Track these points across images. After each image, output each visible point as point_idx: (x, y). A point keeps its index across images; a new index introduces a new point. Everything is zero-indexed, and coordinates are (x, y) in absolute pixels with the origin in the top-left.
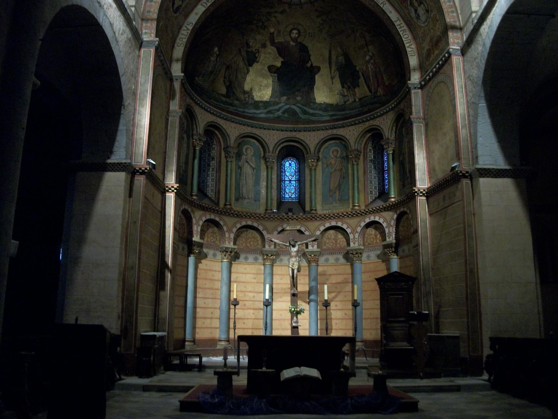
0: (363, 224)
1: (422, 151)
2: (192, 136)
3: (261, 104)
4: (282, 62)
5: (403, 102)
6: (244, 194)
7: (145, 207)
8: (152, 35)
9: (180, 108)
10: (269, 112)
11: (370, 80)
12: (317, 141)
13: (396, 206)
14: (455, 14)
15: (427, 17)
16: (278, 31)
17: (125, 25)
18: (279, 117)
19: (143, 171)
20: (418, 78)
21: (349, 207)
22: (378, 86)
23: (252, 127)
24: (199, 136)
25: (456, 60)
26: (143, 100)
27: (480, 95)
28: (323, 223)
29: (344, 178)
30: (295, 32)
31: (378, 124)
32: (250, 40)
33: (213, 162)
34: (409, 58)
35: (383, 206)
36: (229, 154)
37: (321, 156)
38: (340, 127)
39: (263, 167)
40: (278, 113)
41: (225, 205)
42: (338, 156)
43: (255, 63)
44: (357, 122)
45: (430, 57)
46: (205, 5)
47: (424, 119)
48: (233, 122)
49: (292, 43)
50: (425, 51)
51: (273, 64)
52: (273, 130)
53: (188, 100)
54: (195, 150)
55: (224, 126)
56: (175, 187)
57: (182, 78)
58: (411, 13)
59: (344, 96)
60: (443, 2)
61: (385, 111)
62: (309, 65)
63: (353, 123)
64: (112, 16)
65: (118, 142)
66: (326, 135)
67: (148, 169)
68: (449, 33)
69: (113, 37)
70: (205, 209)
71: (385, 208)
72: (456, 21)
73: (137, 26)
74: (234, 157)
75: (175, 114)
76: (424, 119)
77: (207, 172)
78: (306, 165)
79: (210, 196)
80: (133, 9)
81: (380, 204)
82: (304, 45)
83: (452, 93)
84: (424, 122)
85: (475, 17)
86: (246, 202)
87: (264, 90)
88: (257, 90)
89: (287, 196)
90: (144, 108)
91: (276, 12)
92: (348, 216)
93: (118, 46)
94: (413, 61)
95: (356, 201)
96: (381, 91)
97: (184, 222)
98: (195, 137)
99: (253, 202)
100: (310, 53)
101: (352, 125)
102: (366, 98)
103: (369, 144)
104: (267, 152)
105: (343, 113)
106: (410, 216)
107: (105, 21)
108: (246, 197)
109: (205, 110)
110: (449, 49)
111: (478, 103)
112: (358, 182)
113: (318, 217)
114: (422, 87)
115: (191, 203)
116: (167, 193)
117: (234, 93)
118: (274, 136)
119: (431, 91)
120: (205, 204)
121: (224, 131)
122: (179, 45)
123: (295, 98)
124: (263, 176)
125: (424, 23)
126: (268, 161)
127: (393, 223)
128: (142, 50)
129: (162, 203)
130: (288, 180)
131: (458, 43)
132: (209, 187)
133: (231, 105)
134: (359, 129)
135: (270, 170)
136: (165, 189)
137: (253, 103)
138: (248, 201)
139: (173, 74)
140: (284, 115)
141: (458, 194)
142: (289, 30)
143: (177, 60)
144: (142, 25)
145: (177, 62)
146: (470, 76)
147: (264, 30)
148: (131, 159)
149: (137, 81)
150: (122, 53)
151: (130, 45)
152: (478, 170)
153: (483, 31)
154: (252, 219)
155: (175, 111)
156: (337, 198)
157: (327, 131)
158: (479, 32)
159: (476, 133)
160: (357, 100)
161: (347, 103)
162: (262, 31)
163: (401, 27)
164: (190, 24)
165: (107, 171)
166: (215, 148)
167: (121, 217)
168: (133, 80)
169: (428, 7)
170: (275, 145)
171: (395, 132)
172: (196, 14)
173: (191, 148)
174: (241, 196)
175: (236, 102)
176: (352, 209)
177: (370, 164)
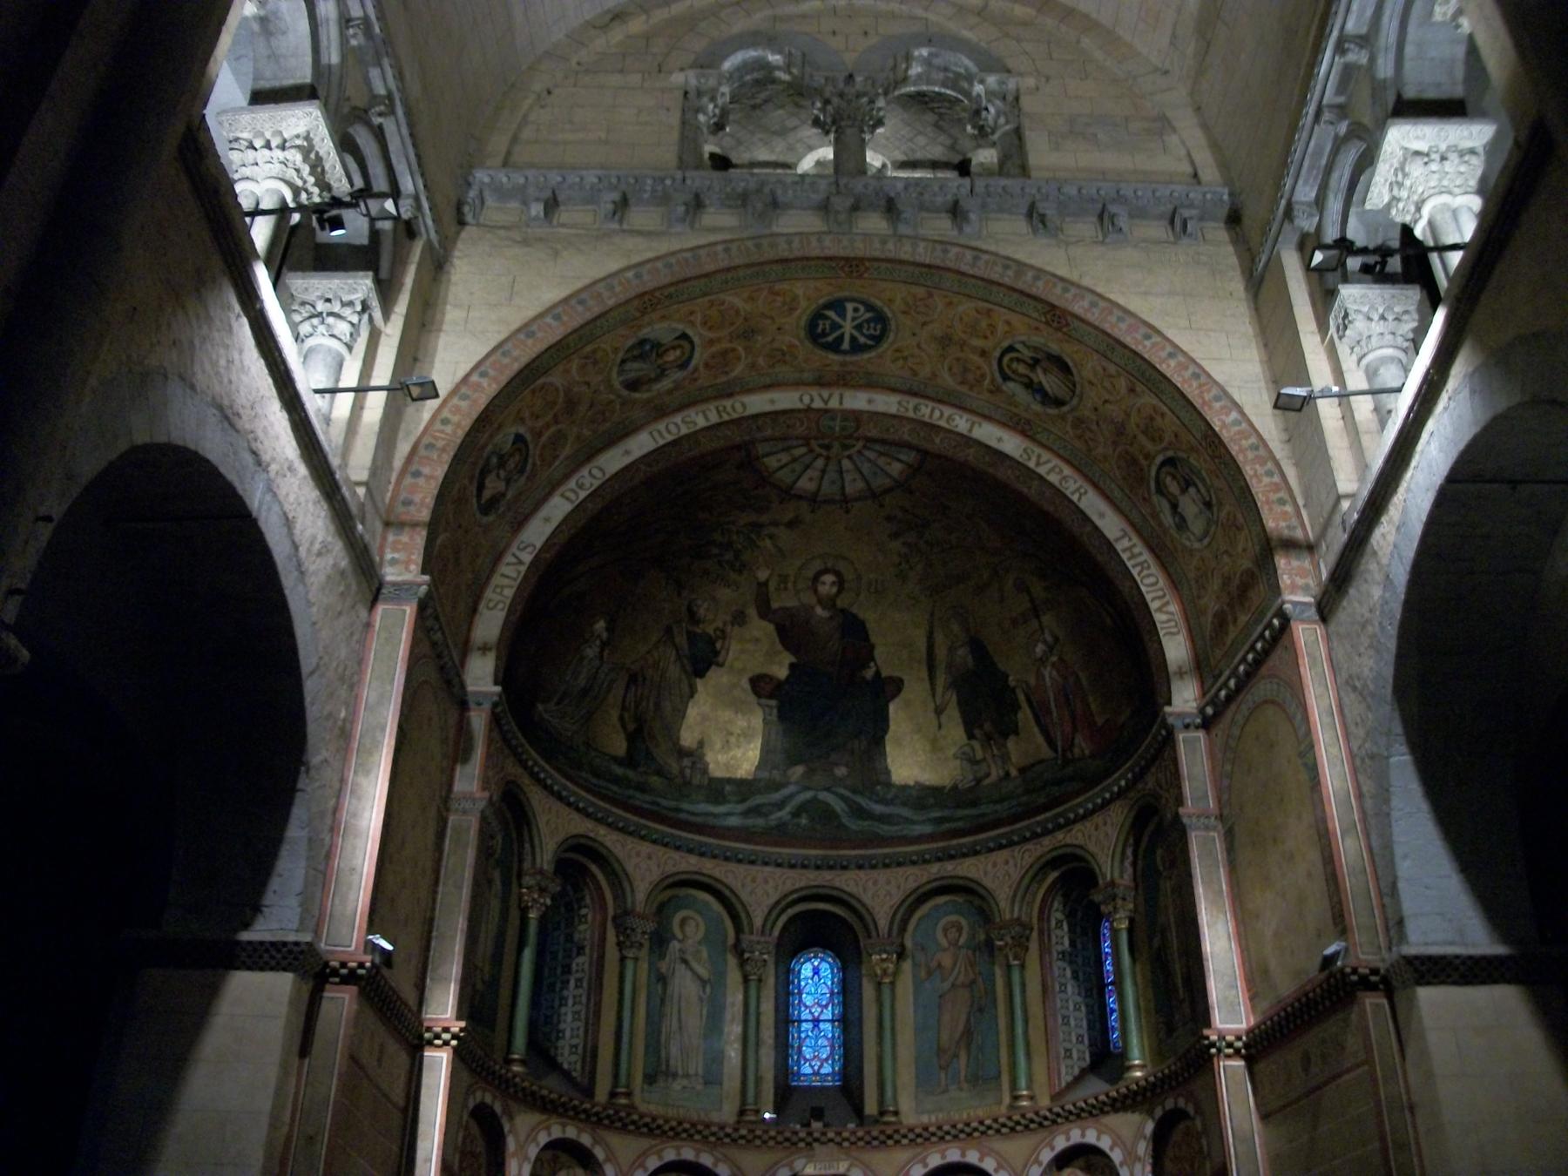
0: (1047, 1156)
1: (1222, 916)
2: (520, 876)
4: (792, 666)
5: (1153, 770)
6: (672, 1062)
7: (349, 1087)
8: (413, 567)
9: (484, 789)
10: (756, 811)
11: (1049, 712)
12: (896, 899)
13: (1149, 1094)
14: (1289, 508)
15: (1209, 522)
16: (780, 576)
17: (332, 528)
18: (782, 826)
19: (352, 972)
20: (1192, 697)
21: (1000, 1103)
22: (1075, 729)
23: (702, 855)
24: (539, 877)
25: (1306, 635)
26: (370, 753)
27: (1390, 730)
28: (919, 1154)
29: (981, 1010)
30: (829, 578)
31: (1082, 843)
32: (699, 602)
33: (581, 959)
34: (1165, 640)
35: (1107, 1095)
36: (628, 936)
37: (909, 944)
38: (965, 855)
39: (734, 976)
40: (779, 814)
41: (613, 1095)
42: (962, 941)
43: (713, 667)
44: (1016, 838)
45: (1227, 634)
46: (572, 496)
47: (1221, 817)
48: (643, 838)
49: (819, 611)
50: (1210, 619)
51: (765, 670)
52: (766, 864)
53: (513, 769)
54: (524, 920)
55: (618, 850)
56: (455, 1030)
57: (496, 698)
59: (973, 762)
60: (1251, 478)
61: (1099, 801)
62: (869, 674)
63: (1004, 842)
64: (292, 498)
65: (281, 876)
66: (925, 880)
67: (368, 964)
68: (1277, 558)
69: (289, 558)
70: (549, 1106)
71: (1115, 1100)
72: (1295, 528)
73: (367, 537)
74: (647, 945)
75: (468, 805)
76: (1221, 815)
77: (562, 989)
78: (864, 972)
79: (566, 1066)
80: (361, 491)
81: (1096, 1088)
82: (854, 616)
83: (1302, 731)
84: (1220, 827)
85: (1350, 510)
86: (679, 1088)
87: (739, 747)
88: (718, 746)
89: (806, 1069)
90: (372, 776)
91: (775, 524)
92: (998, 1131)
93: (305, 585)
94: (1176, 649)
95: (1023, 1082)
96: (1083, 745)
97: (480, 1147)
98: (528, 880)
99: (699, 1087)
100: (873, 639)
101: (1001, 847)
103: (1056, 905)
104: (746, 929)
105: (974, 812)
106: (1198, 1123)
107: (269, 509)
108: (680, 1072)
109: (560, 798)
110: (1283, 603)
111: (1386, 754)
112: (1026, 1021)
113: (905, 1136)
114: (1207, 724)
115: (504, 1086)
116: (427, 1048)
118: (766, 882)
119: (1236, 732)
120: (550, 1092)
121: (616, 865)
122: (491, 605)
124: (733, 1004)
125: (1201, 540)
127: (1143, 1148)
128: (380, 608)
129: (410, 1080)
130: (810, 1017)
131: (1306, 589)
132: (563, 1037)
133: (642, 788)
135: (753, 985)
136: (421, 1037)
137: (706, 782)
138: (685, 1082)
139: (470, 688)
140: (796, 820)
141: (1352, 1043)
142: (810, 573)
143: (484, 649)
144: (384, 538)
145: (484, 654)
146: (1351, 676)
147: (740, 572)
148: (317, 932)
149: (356, 697)
150: (314, 609)
151: (342, 588)
152: (1410, 961)
153: (1382, 542)
154: (697, 1141)
155: (469, 797)
156: (963, 1073)
157: (927, 867)
158: (1369, 547)
159: (1388, 846)
160: (1014, 772)
161: (987, 782)
162: (733, 576)
163: (1133, 557)
164: (525, 548)
165: (238, 968)
167: (264, 1121)
168: (343, 692)
171: (1134, 864)
172: (547, 520)
173: (514, 914)
174: (664, 1067)
175: (655, 781)
176: (1012, 1107)
177: (1060, 963)
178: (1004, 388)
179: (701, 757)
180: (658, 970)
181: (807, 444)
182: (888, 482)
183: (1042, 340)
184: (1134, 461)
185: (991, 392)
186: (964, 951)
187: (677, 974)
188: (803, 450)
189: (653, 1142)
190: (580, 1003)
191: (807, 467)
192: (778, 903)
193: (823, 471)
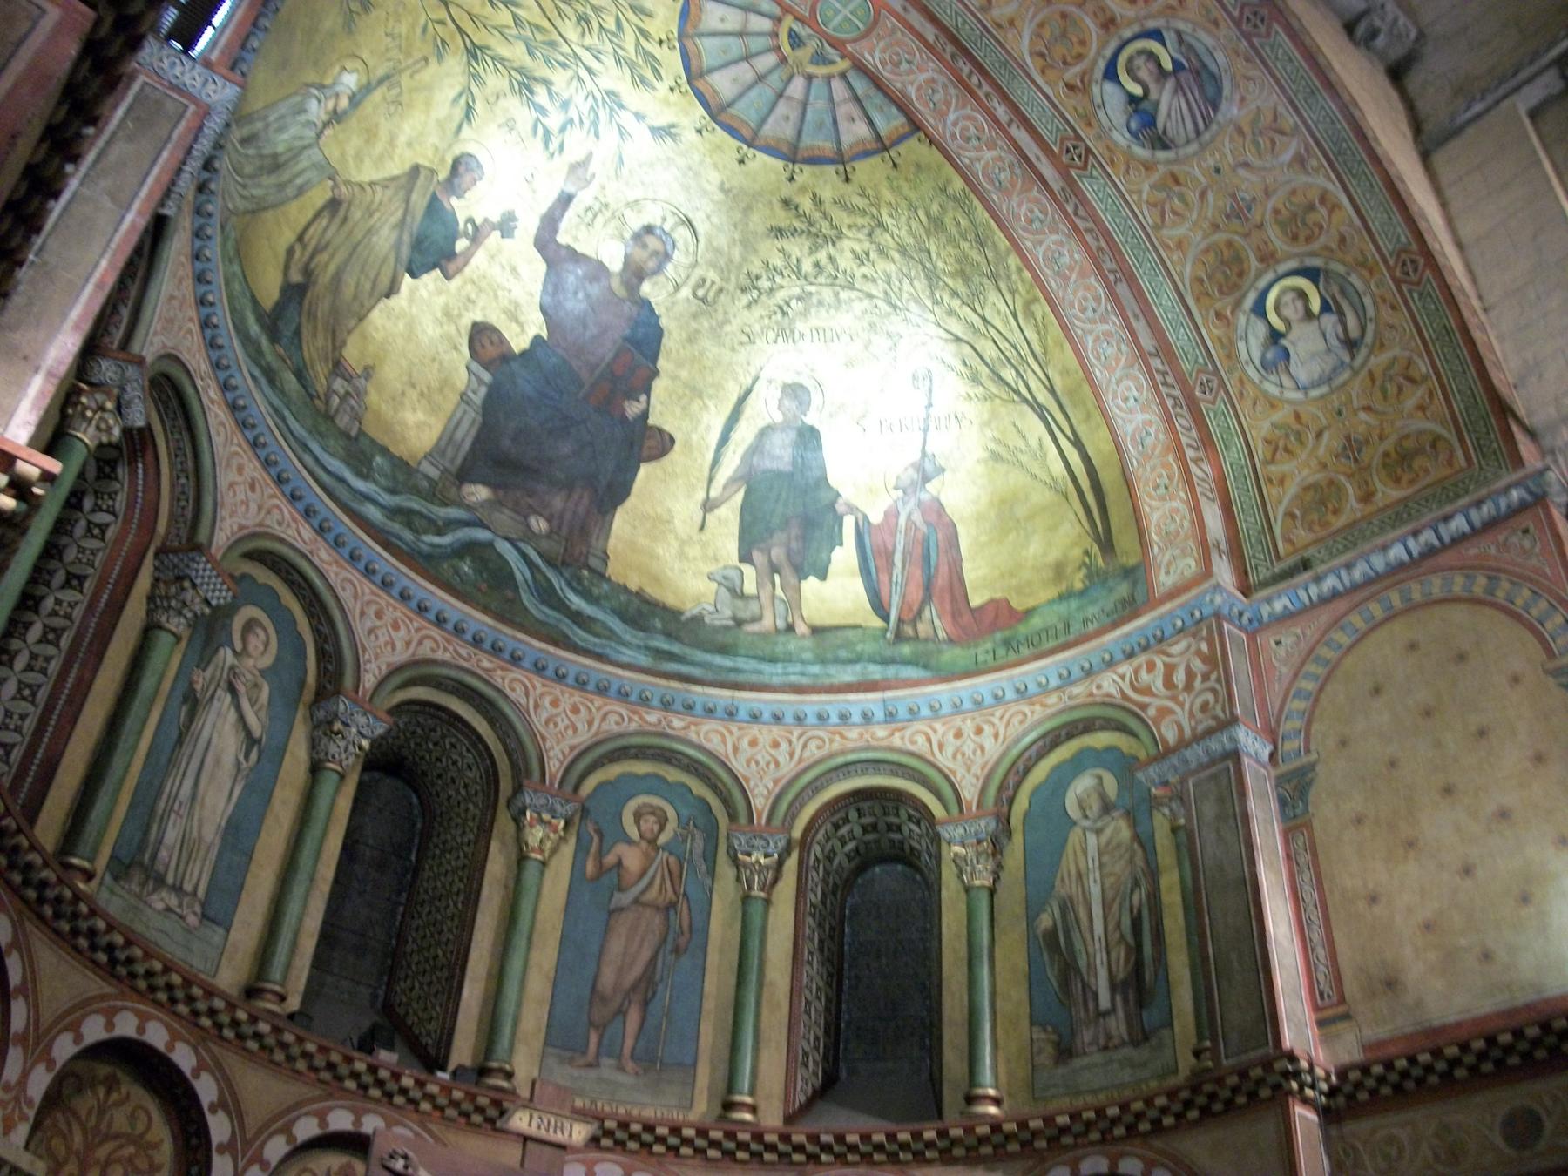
3: (378, 460)
6: (163, 853)
11: (891, 564)
12: (583, 737)
22: (923, 603)
29: (677, 951)
31: (921, 745)
33: (69, 596)
40: (437, 540)
42: (662, 840)
43: (438, 271)
49: (616, 284)
58: (1241, 345)
66: (633, 727)
86: (160, 906)
92: (700, 1152)
99: (192, 920)
100: (662, 363)
102: (851, 634)
103: (820, 836)
108: (170, 879)
117: (298, 333)
123: (526, 517)
126: (339, 732)
134: (805, 746)
137: (353, 433)
138: (173, 901)
154: (179, 1016)
160: (801, 628)
161: (754, 628)
166: (110, 533)
169: (1363, 329)
170: (391, 674)
178: (1096, 89)
179: (360, 394)
180: (191, 683)
181: (778, 20)
182: (828, 147)
183: (1208, 40)
184: (1237, 261)
185: (1071, 87)
186: (663, 855)
187: (216, 703)
188: (765, 25)
189: (108, 990)
190: (44, 671)
191: (747, 58)
192: (401, 668)
193: (760, 78)
